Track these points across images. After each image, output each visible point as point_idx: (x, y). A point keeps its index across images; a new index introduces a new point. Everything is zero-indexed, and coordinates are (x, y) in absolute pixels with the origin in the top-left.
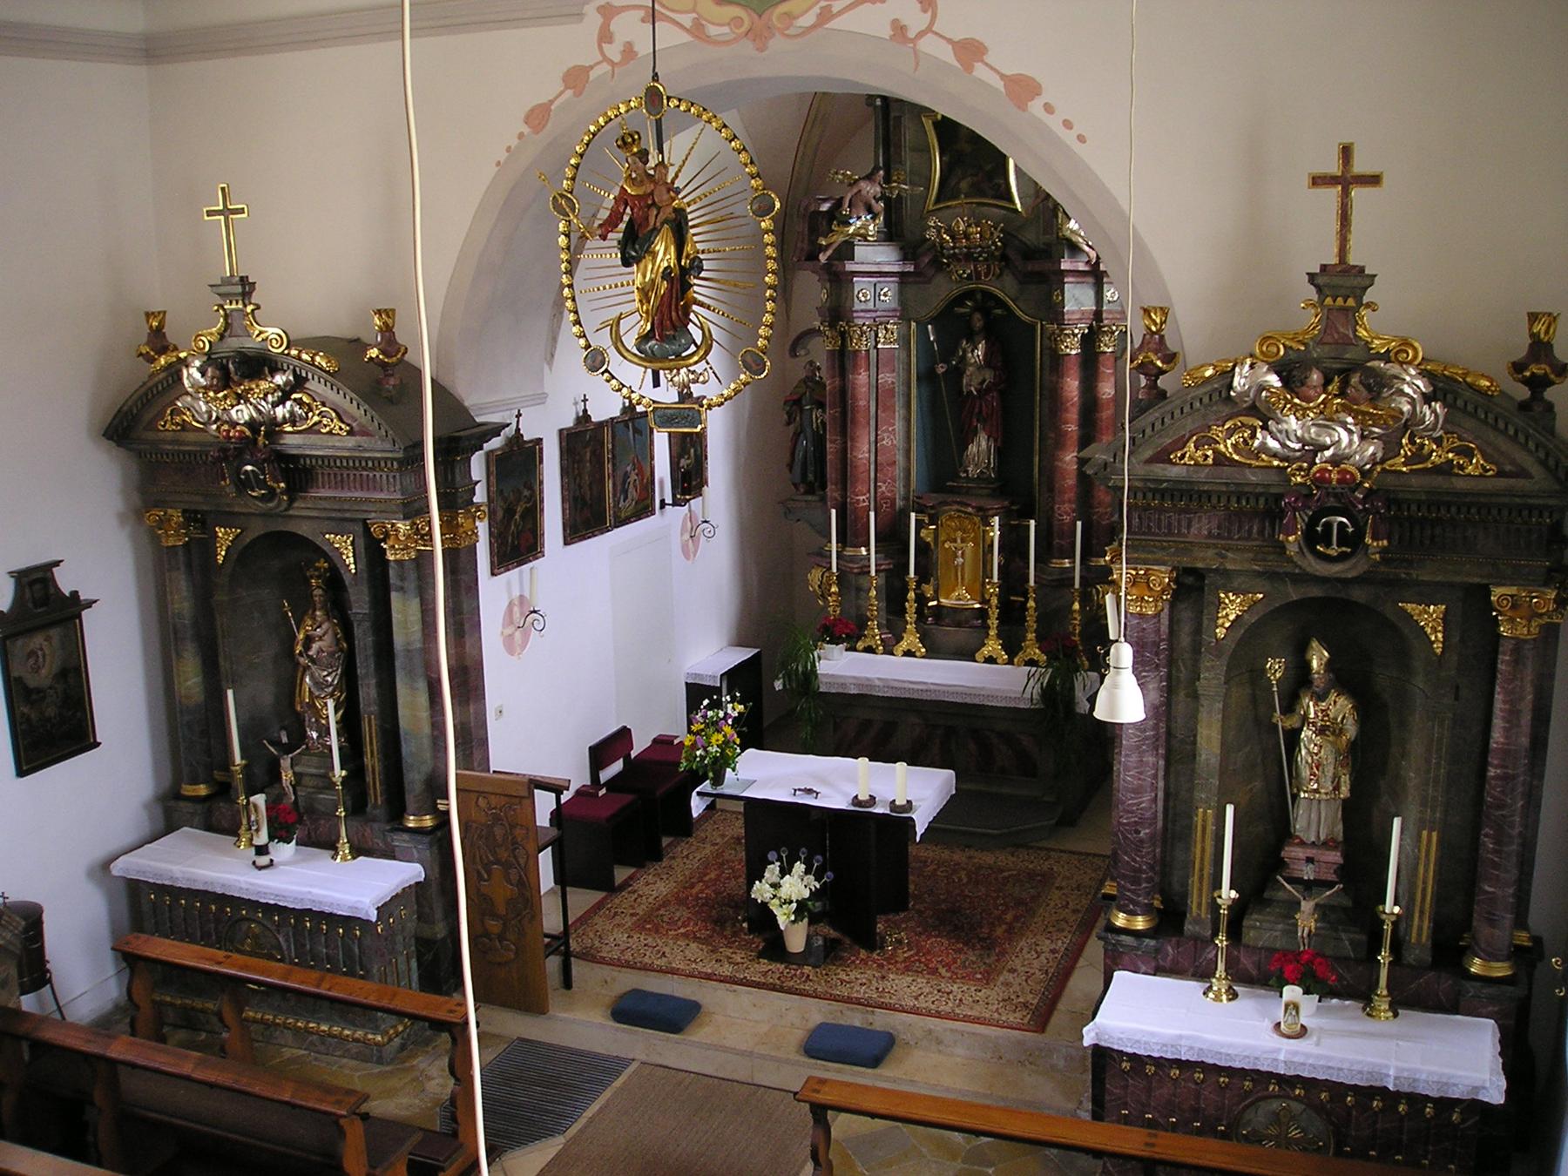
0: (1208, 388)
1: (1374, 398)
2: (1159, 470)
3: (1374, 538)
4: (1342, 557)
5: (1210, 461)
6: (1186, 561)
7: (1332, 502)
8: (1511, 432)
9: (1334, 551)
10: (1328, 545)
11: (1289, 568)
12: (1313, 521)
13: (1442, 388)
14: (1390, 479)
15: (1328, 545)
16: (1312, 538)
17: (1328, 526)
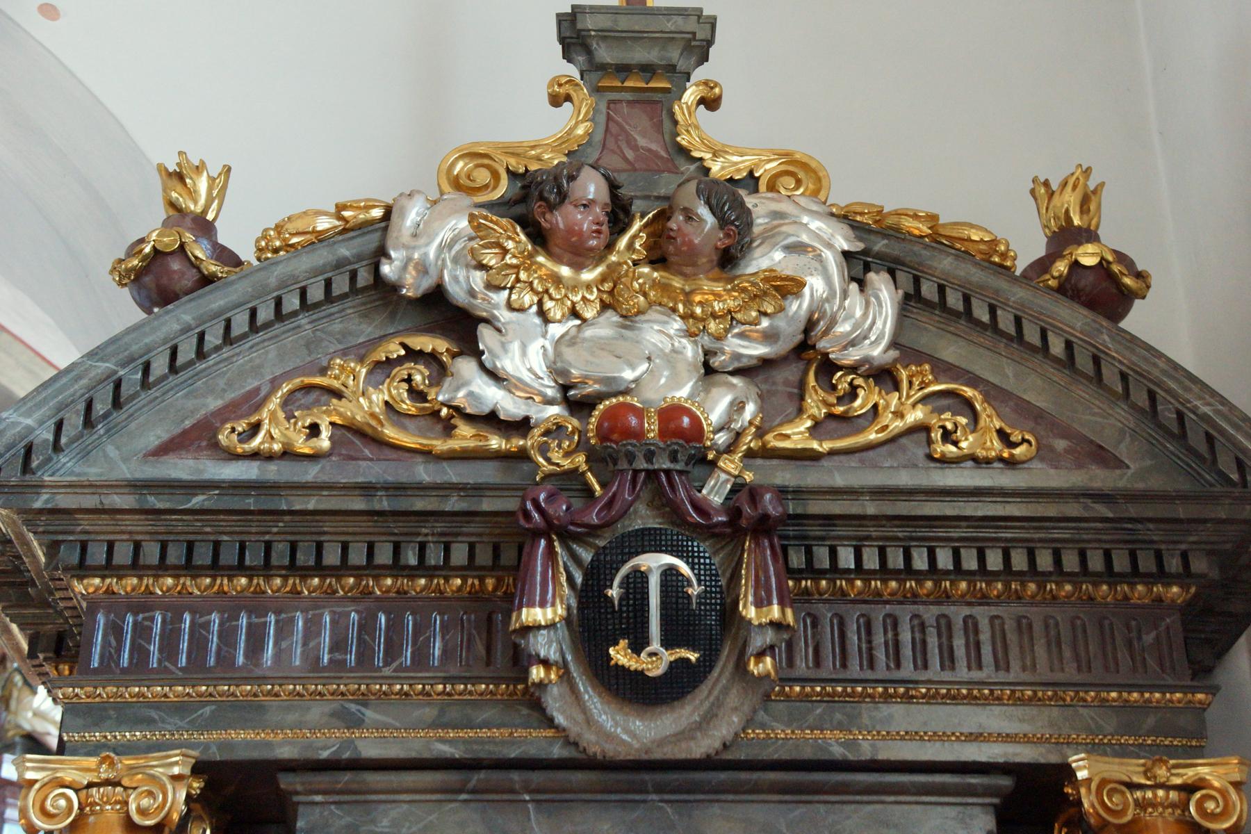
0: (323, 256)
1: (728, 259)
2: (181, 468)
3: (759, 604)
4: (676, 685)
5: (324, 442)
6: (244, 741)
7: (644, 518)
8: (1057, 347)
9: (655, 660)
10: (638, 645)
11: (532, 741)
12: (597, 576)
13: (878, 249)
14: (785, 476)
15: (638, 645)
16: (600, 622)
17: (638, 581)
